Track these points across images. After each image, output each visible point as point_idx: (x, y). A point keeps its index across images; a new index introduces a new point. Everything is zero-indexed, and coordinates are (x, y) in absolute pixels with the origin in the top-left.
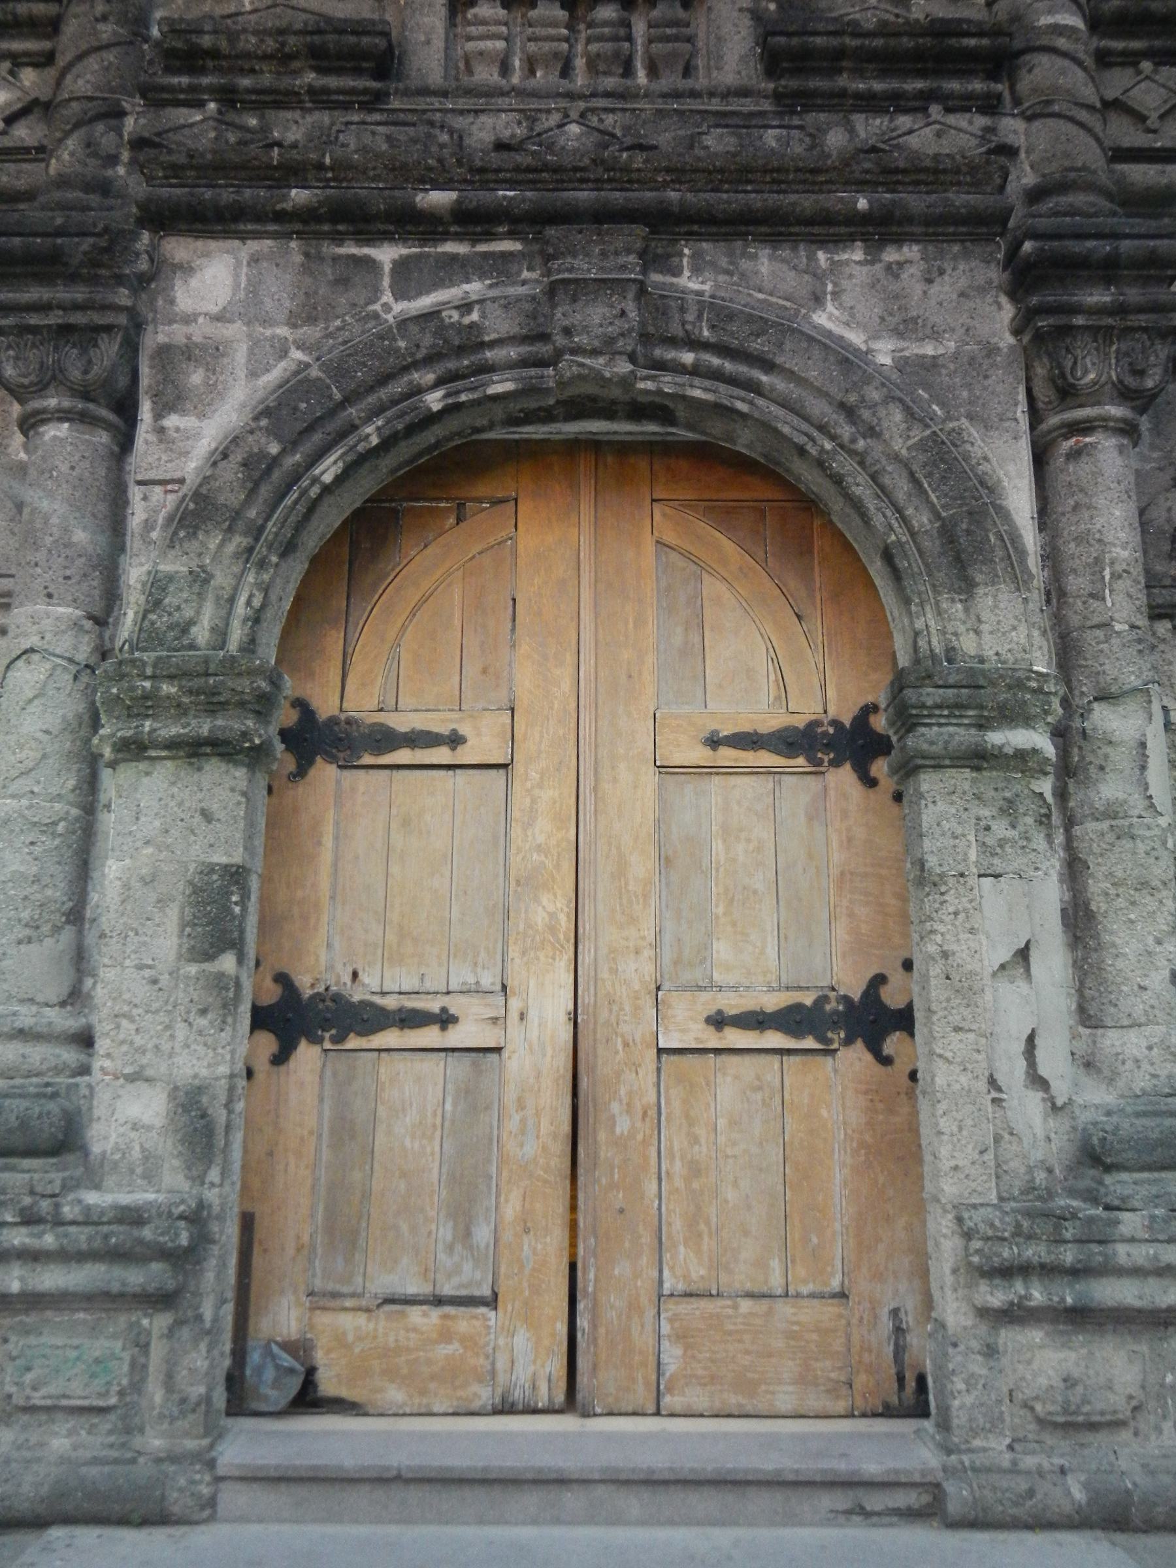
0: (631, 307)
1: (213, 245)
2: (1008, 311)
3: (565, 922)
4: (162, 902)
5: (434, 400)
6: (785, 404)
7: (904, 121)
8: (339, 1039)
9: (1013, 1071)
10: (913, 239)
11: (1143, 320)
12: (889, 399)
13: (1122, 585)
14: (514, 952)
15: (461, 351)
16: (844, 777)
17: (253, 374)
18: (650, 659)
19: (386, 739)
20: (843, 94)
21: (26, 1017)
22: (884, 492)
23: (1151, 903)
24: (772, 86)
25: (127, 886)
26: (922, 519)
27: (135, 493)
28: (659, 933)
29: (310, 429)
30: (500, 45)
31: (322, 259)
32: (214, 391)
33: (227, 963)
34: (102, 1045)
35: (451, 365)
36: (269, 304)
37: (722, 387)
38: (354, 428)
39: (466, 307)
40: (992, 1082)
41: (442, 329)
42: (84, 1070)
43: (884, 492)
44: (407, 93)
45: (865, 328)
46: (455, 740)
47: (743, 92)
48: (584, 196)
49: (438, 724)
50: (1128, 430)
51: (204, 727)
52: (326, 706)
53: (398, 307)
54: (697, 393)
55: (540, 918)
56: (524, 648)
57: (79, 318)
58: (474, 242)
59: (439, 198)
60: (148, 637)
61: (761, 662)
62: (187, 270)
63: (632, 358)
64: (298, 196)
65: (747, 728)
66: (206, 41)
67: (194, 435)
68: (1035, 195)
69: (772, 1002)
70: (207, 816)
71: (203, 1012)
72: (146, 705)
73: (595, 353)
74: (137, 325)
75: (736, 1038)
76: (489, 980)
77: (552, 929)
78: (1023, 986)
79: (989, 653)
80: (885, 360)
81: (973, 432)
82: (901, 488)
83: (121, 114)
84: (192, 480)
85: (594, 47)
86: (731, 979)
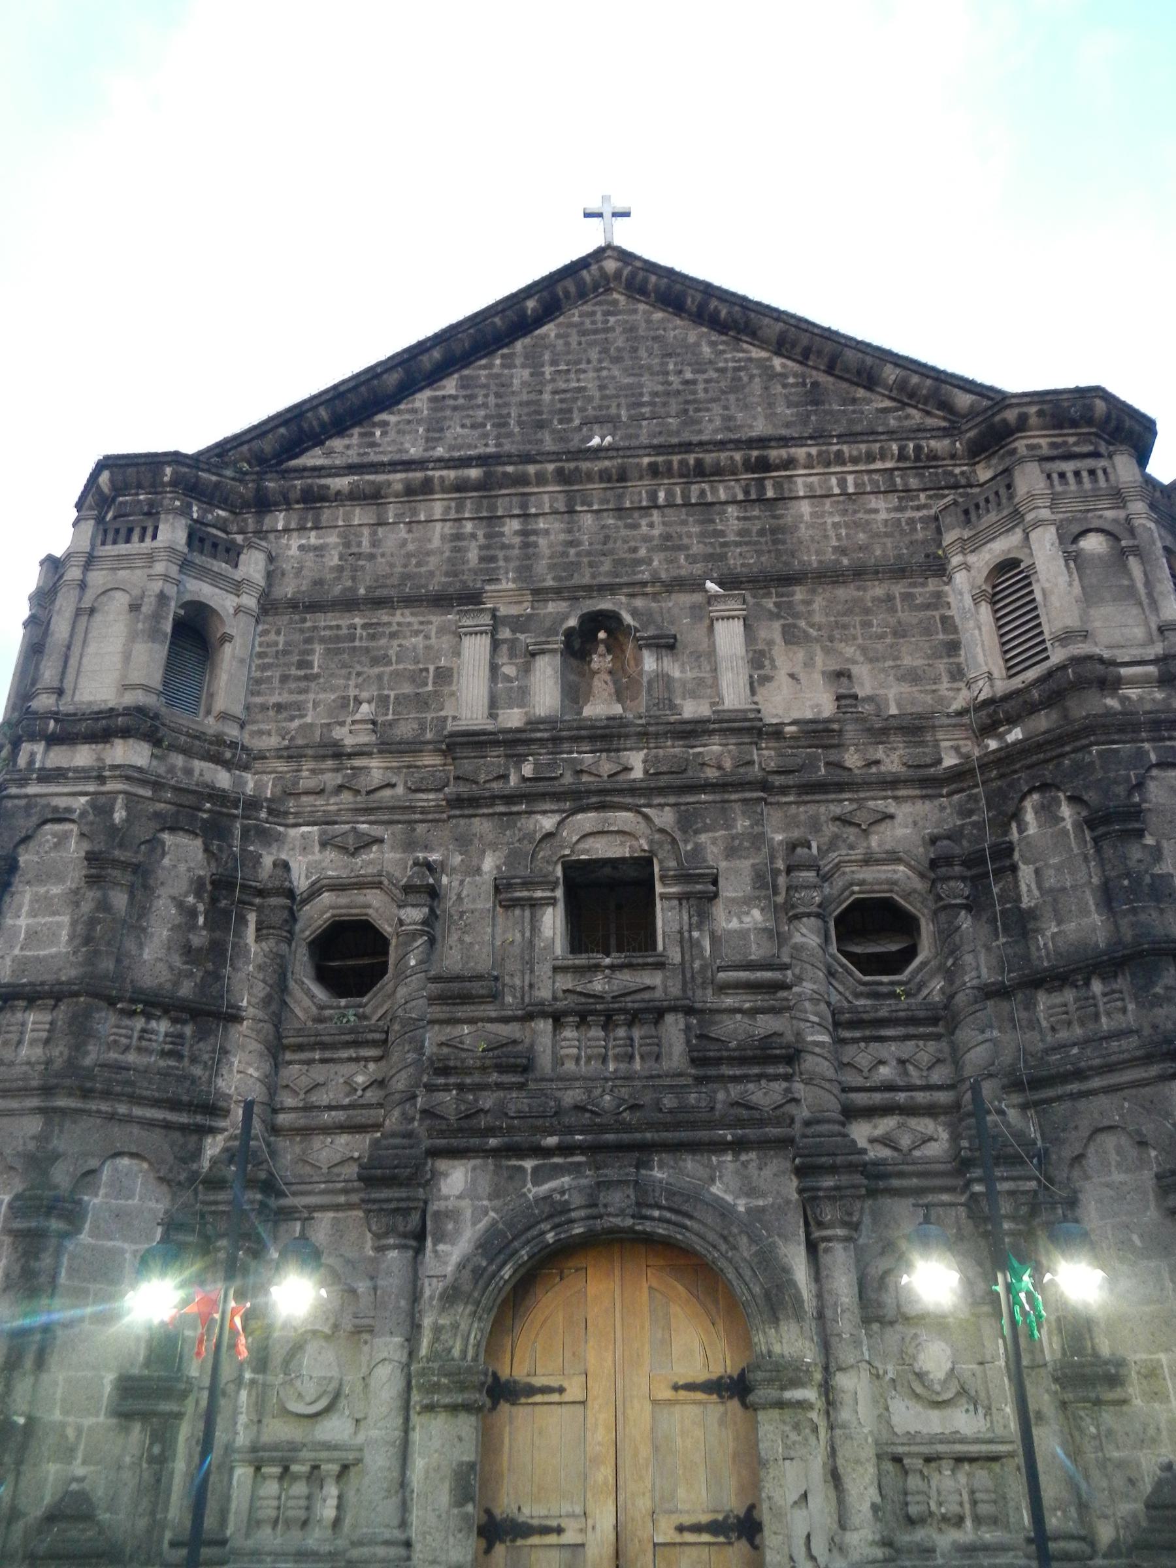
0: (631, 1191)
1: (456, 1162)
2: (795, 1182)
3: (611, 1481)
4: (442, 1479)
5: (550, 1237)
6: (697, 1235)
7: (751, 1086)
8: (513, 1540)
9: (800, 1553)
10: (752, 1149)
11: (848, 1192)
12: (741, 1232)
13: (847, 1315)
14: (589, 1496)
15: (561, 1213)
16: (734, 1404)
17: (474, 1224)
18: (647, 1348)
19: (531, 1390)
20: (723, 1076)
21: (387, 1534)
22: (740, 1276)
23: (861, 1470)
24: (693, 1071)
25: (427, 1472)
26: (757, 1290)
27: (426, 1281)
28: (653, 1485)
29: (500, 1252)
30: (575, 1051)
31: (501, 1167)
32: (458, 1232)
33: (470, 1508)
34: (418, 1547)
35: (557, 1220)
36: (480, 1190)
37: (671, 1227)
38: (516, 1251)
39: (563, 1193)
40: (792, 1559)
41: (553, 1203)
42: (409, 1559)
43: (740, 1276)
44: (536, 1080)
45: (732, 1193)
46: (561, 1390)
47: (680, 1075)
48: (610, 1137)
49: (553, 1382)
50: (848, 1239)
51: (459, 1398)
52: (504, 1374)
53: (534, 1190)
54: (660, 1231)
55: (600, 1478)
56: (591, 1344)
57: (403, 1205)
58: (566, 1156)
59: (552, 1141)
60: (433, 1356)
61: (697, 1345)
62: (446, 1175)
63: (633, 1217)
64: (493, 1142)
65: (690, 1380)
66: (452, 1063)
67: (450, 1254)
68: (808, 1123)
69: (704, 1518)
70: (460, 1439)
71: (460, 1531)
72: (435, 1388)
73: (617, 1215)
74: (426, 1202)
75: (689, 1537)
76: (578, 1510)
77: (606, 1483)
78: (804, 1512)
79: (786, 1353)
80: (741, 1209)
81: (780, 1243)
82: (747, 1274)
83: (414, 1097)
84: (450, 1279)
85: (617, 1050)
86: (687, 1507)
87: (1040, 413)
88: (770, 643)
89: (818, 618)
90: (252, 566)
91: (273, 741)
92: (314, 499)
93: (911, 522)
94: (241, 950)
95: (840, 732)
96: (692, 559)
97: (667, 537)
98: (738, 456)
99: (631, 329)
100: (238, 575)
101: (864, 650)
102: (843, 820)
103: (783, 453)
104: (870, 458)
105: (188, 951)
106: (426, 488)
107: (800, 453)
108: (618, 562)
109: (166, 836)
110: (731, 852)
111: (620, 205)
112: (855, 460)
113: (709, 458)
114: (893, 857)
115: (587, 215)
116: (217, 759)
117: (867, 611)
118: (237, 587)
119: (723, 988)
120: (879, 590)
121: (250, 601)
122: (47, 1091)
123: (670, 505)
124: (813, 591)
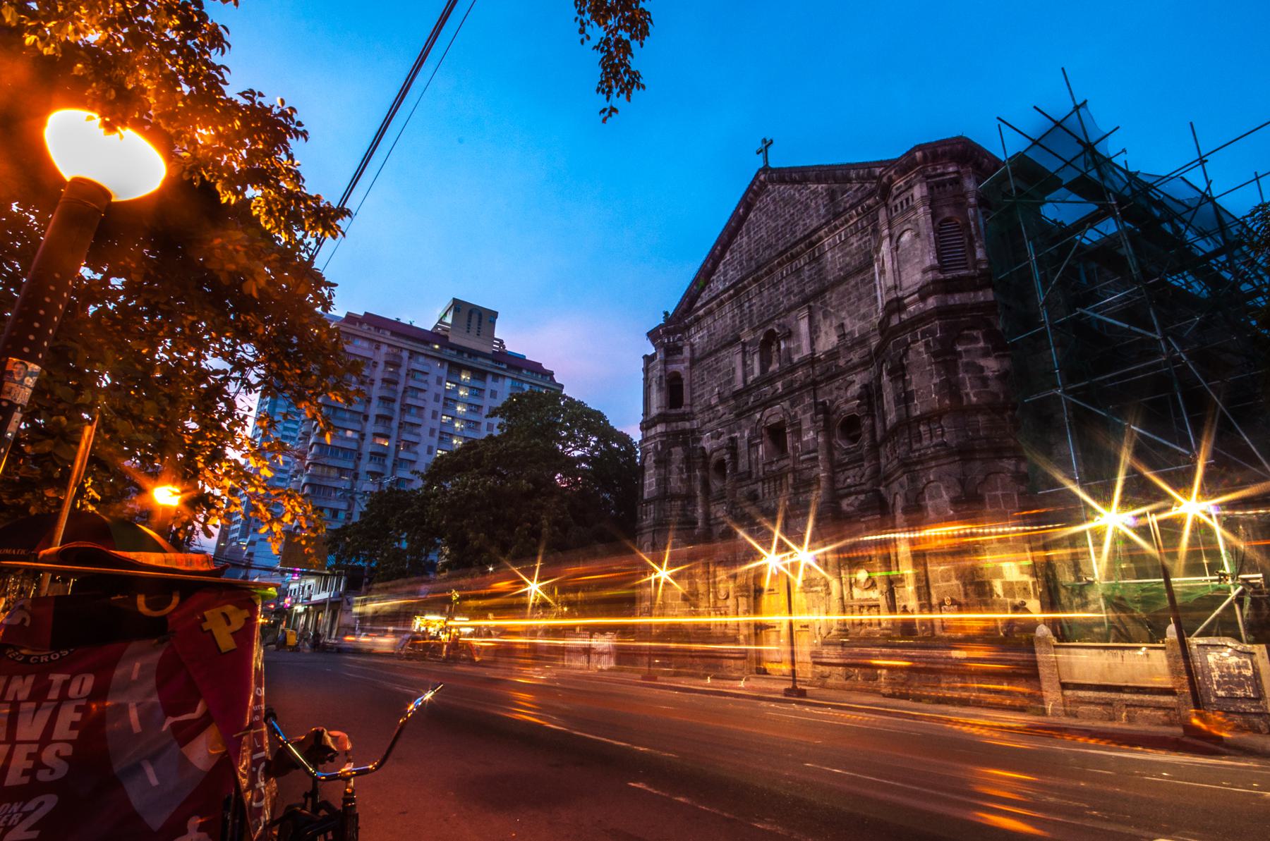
87: (895, 173)
88: (819, 321)
89: (834, 304)
90: (687, 351)
91: (699, 408)
92: (698, 319)
93: (865, 242)
94: (695, 476)
95: (838, 352)
96: (795, 296)
97: (787, 290)
98: (803, 245)
99: (774, 200)
100: (682, 357)
101: (848, 312)
102: (838, 388)
103: (816, 236)
104: (847, 221)
105: (682, 480)
106: (722, 303)
107: (822, 233)
108: (775, 307)
109: (673, 450)
110: (804, 412)
111: (768, 140)
112: (842, 225)
113: (793, 251)
114: (854, 398)
115: (758, 153)
116: (683, 420)
117: (850, 293)
118: (683, 361)
119: (803, 461)
120: (853, 282)
121: (687, 364)
122: (654, 525)
123: (787, 275)
124: (832, 292)
